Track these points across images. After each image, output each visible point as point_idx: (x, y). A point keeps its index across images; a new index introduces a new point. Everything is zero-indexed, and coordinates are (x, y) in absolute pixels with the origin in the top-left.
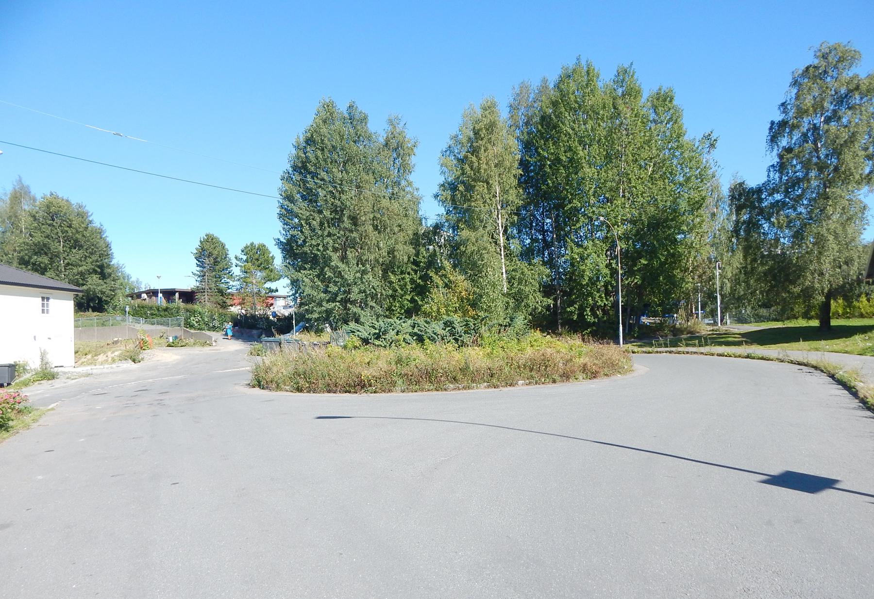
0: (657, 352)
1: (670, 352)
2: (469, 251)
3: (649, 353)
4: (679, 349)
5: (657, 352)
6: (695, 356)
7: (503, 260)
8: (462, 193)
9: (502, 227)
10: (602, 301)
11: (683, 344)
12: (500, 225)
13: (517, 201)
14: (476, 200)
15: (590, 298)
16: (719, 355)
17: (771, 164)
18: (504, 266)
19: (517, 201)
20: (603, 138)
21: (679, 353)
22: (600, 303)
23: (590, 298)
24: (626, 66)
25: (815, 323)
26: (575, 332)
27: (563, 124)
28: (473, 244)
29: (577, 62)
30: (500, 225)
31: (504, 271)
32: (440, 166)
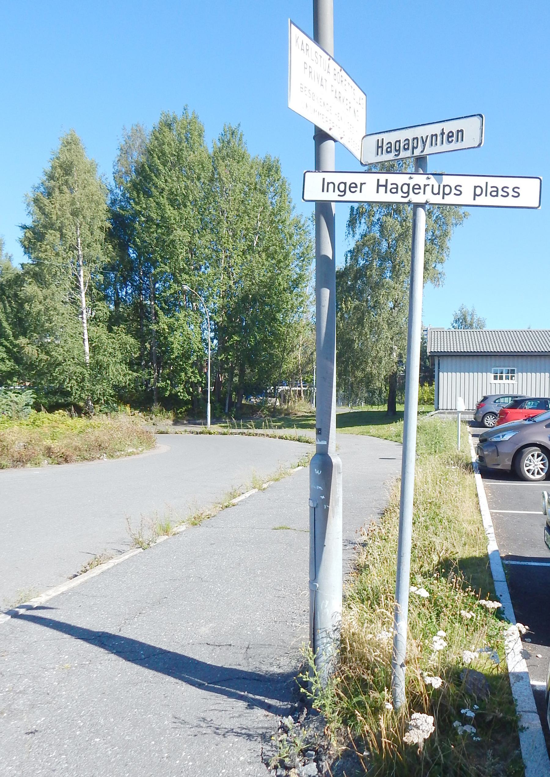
0: (231, 434)
1: (242, 434)
2: (35, 310)
3: (224, 434)
4: (251, 431)
5: (231, 434)
6: (261, 438)
7: (85, 325)
8: (30, 241)
9: (85, 284)
10: (195, 377)
11: (251, 425)
12: (82, 283)
13: (103, 258)
14: (46, 251)
15: (183, 374)
16: (281, 438)
17: (349, 250)
18: (86, 332)
19: (103, 258)
20: (198, 199)
21: (249, 435)
22: (193, 379)
23: (183, 374)
24: (234, 127)
25: (384, 408)
26: (168, 410)
27: (156, 177)
28: (40, 303)
29: (184, 112)
30: (82, 283)
31: (86, 337)
32: (25, 205)
